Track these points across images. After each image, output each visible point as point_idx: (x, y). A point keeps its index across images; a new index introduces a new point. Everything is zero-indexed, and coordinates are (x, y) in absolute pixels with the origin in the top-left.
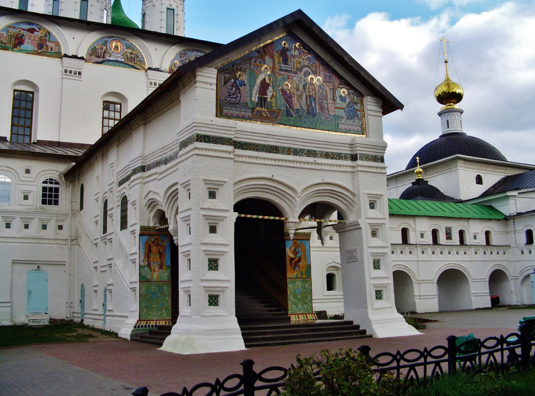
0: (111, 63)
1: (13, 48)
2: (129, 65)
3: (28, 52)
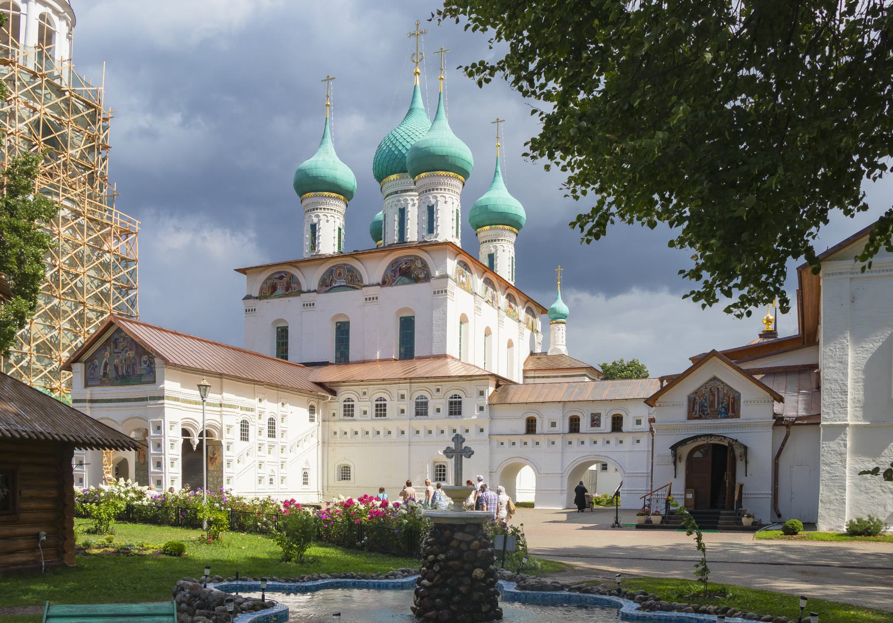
0: (336, 289)
2: (351, 287)
3: (280, 297)
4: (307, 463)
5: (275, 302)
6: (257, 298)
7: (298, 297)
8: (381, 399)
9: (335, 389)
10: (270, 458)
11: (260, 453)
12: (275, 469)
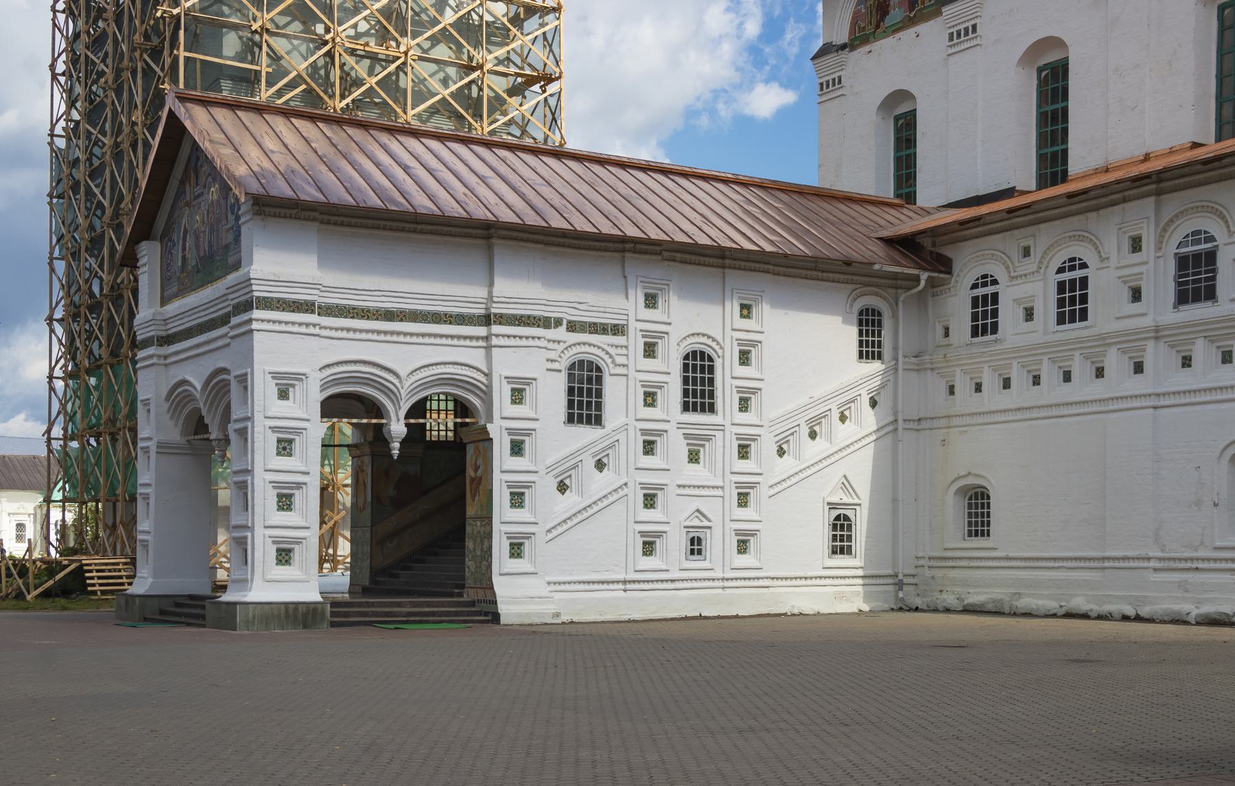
1: (875, 32)
3: (897, 29)
4: (846, 484)
5: (885, 47)
6: (843, 47)
7: (939, 19)
8: (1074, 264)
9: (948, 251)
10: (696, 474)
11: (648, 461)
12: (712, 508)
